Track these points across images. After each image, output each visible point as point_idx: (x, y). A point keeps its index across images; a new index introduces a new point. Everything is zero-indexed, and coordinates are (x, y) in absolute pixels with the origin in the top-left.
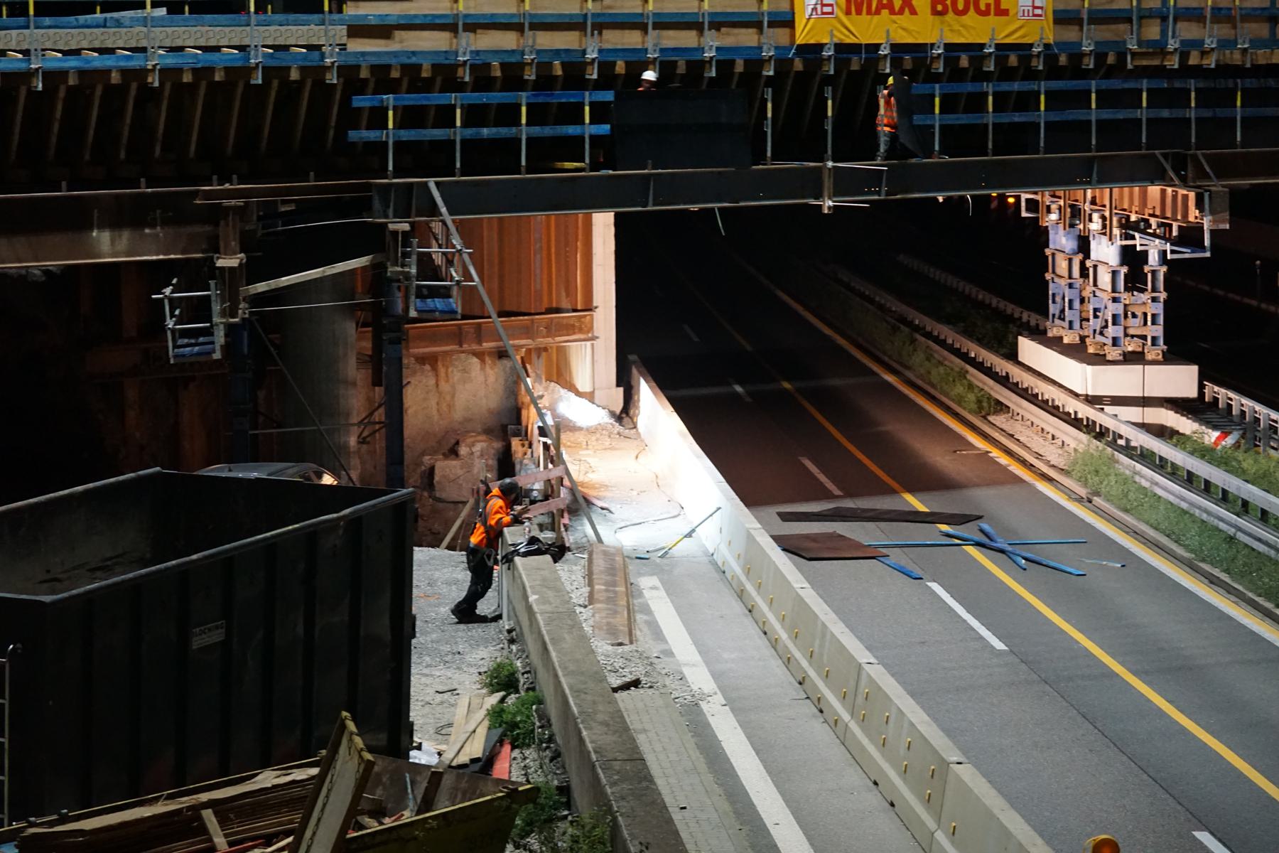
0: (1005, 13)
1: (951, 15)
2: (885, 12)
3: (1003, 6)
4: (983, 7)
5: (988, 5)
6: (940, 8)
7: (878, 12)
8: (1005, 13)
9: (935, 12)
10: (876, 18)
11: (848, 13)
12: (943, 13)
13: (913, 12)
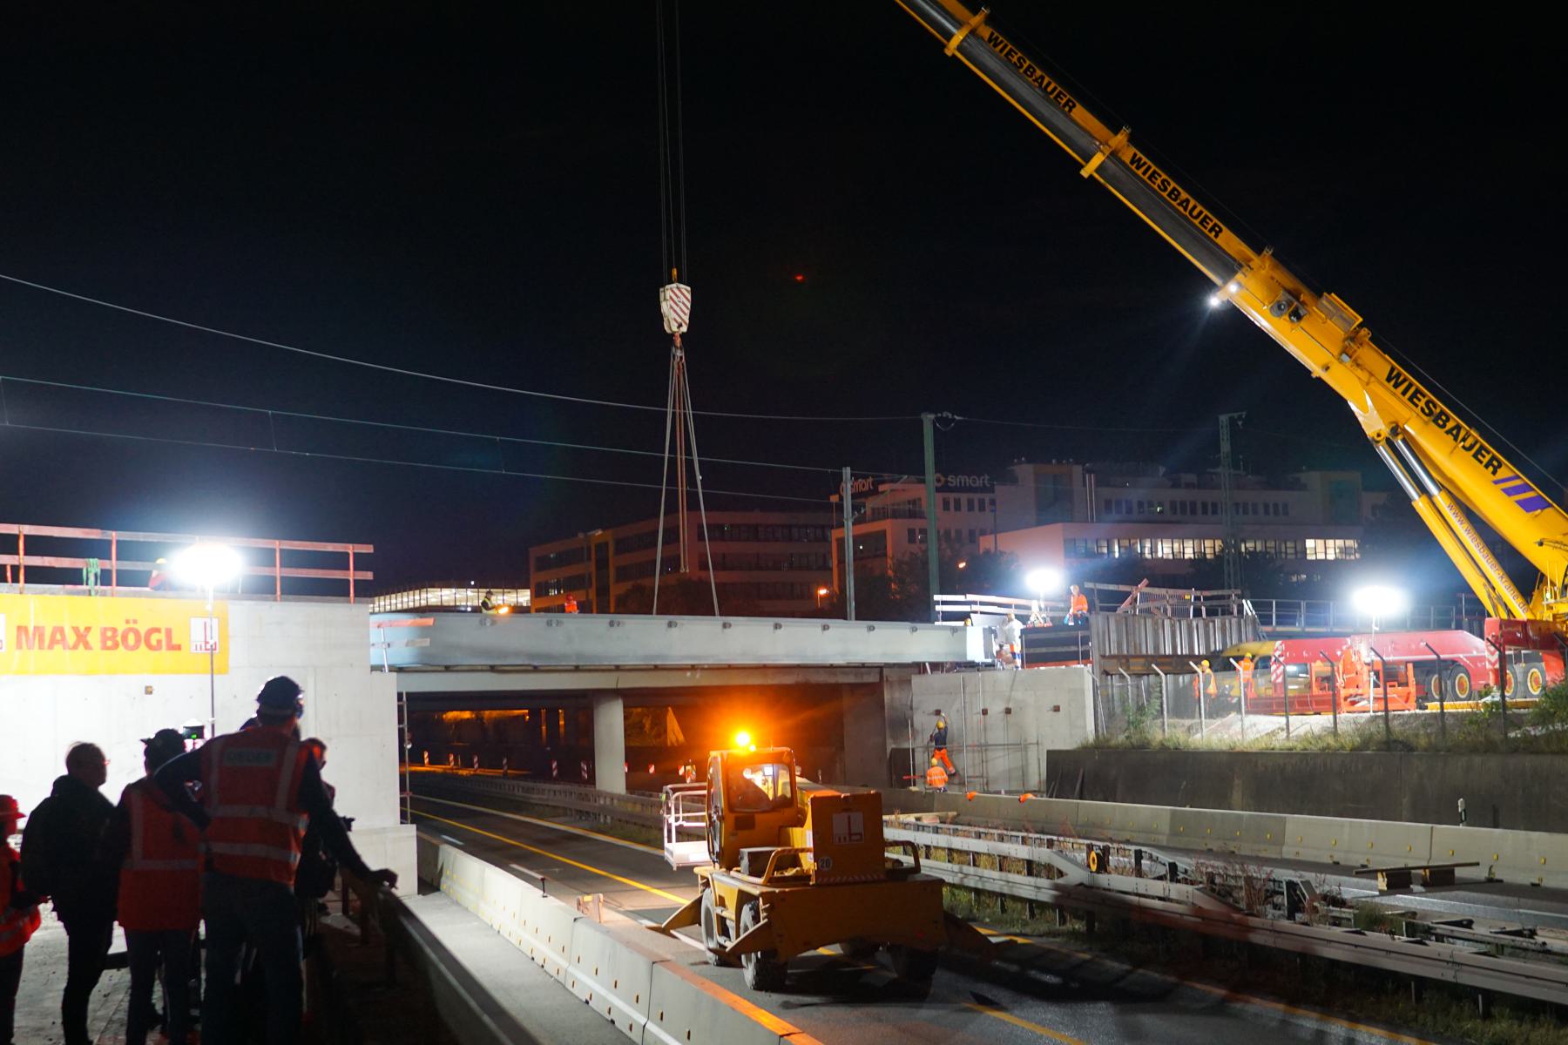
0: (179, 648)
1: (121, 647)
2: (58, 648)
3: (175, 641)
4: (154, 642)
5: (159, 642)
6: (109, 643)
7: (51, 647)
8: (179, 648)
9: (105, 647)
10: (46, 652)
11: (19, 646)
12: (116, 646)
13: (87, 646)
